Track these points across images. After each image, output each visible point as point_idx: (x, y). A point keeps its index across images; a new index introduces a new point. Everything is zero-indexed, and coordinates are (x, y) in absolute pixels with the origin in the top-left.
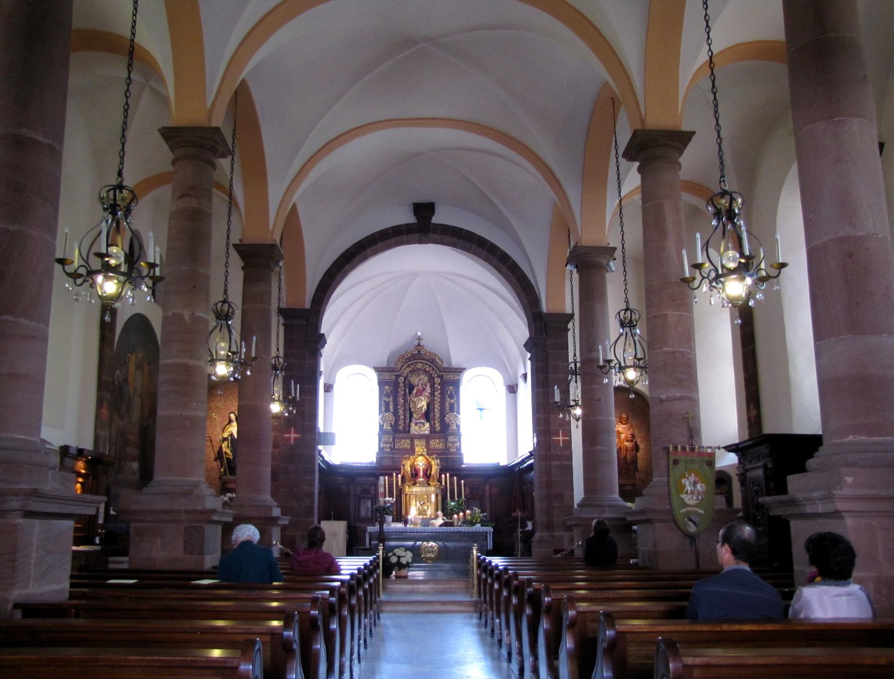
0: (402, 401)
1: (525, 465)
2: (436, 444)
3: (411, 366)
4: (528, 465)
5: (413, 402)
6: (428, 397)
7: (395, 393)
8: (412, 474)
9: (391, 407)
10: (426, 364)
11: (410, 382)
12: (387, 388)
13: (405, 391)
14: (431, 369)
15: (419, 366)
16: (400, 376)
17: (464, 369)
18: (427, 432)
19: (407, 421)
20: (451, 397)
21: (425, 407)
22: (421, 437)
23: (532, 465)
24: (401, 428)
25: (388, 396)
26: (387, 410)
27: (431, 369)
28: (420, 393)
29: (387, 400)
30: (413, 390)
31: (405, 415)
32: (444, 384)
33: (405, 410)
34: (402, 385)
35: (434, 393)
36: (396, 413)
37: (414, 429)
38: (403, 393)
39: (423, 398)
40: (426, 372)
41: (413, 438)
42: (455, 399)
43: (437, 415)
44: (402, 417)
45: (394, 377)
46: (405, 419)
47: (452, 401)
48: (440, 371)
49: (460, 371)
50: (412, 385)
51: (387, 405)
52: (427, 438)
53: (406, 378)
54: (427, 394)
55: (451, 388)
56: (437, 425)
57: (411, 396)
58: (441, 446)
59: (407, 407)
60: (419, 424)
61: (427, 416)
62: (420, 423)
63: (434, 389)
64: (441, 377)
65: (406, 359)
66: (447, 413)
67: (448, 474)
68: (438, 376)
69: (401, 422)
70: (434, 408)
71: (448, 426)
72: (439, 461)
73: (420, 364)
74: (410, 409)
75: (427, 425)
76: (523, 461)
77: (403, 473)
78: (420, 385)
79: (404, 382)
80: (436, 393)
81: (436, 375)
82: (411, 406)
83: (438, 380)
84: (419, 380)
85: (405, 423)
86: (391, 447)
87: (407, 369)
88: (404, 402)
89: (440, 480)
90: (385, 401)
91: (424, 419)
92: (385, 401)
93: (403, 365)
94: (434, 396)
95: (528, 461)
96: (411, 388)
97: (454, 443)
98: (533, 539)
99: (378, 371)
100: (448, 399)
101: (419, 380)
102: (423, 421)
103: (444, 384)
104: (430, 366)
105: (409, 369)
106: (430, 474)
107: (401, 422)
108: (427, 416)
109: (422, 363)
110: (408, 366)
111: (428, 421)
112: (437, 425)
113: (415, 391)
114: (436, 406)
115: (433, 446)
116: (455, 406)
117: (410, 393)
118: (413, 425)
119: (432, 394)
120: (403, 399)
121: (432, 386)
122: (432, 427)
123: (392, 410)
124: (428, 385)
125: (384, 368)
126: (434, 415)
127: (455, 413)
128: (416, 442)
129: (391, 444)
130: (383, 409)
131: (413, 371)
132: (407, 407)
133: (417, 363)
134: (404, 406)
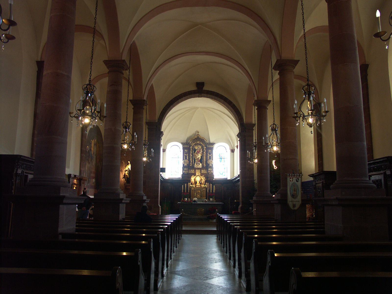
0: (192, 155)
1: (237, 180)
2: (203, 171)
3: (195, 142)
4: (238, 180)
5: (196, 156)
6: (201, 154)
8: (195, 183)
10: (201, 142)
11: (194, 148)
13: (193, 152)
14: (202, 143)
15: (198, 142)
17: (215, 143)
18: (200, 167)
19: (193, 163)
20: (210, 154)
21: (200, 158)
22: (198, 169)
23: (239, 179)
25: (186, 153)
26: (186, 159)
27: (202, 143)
28: (198, 152)
29: (186, 155)
30: (196, 151)
31: (192, 161)
33: (192, 159)
35: (203, 153)
36: (189, 160)
38: (192, 152)
39: (199, 154)
40: (200, 145)
41: (195, 169)
42: (211, 155)
43: (205, 160)
44: (192, 161)
46: (192, 162)
47: (210, 155)
48: (206, 144)
49: (213, 144)
50: (195, 149)
51: (186, 156)
53: (193, 147)
54: (201, 153)
55: (210, 150)
57: (195, 153)
59: (193, 158)
60: (198, 164)
61: (201, 161)
62: (198, 163)
63: (203, 150)
64: (206, 146)
65: (194, 140)
66: (208, 160)
67: (208, 183)
69: (191, 163)
70: (203, 158)
71: (209, 165)
72: (205, 178)
73: (198, 142)
74: (194, 158)
75: (201, 164)
76: (236, 178)
77: (191, 183)
78: (198, 149)
79: (192, 149)
80: (204, 152)
81: (204, 146)
82: (195, 157)
83: (205, 148)
84: (198, 148)
85: (192, 163)
86: (187, 172)
87: (194, 143)
88: (192, 156)
90: (185, 155)
91: (199, 162)
92: (185, 155)
93: (192, 142)
94: (204, 154)
95: (238, 178)
96: (195, 150)
97: (210, 171)
98: (239, 207)
99: (183, 144)
100: (209, 155)
101: (198, 148)
102: (199, 163)
103: (208, 149)
104: (202, 142)
106: (201, 183)
107: (191, 163)
108: (201, 161)
109: (199, 141)
110: (194, 142)
113: (196, 152)
114: (204, 157)
115: (203, 172)
116: (211, 157)
117: (194, 152)
118: (195, 164)
119: (203, 153)
120: (192, 155)
122: (203, 165)
123: (188, 159)
124: (201, 150)
125: (185, 143)
126: (203, 161)
127: (211, 160)
128: (197, 171)
129: (187, 171)
131: (196, 145)
132: (193, 158)
133: (197, 141)
134: (192, 157)
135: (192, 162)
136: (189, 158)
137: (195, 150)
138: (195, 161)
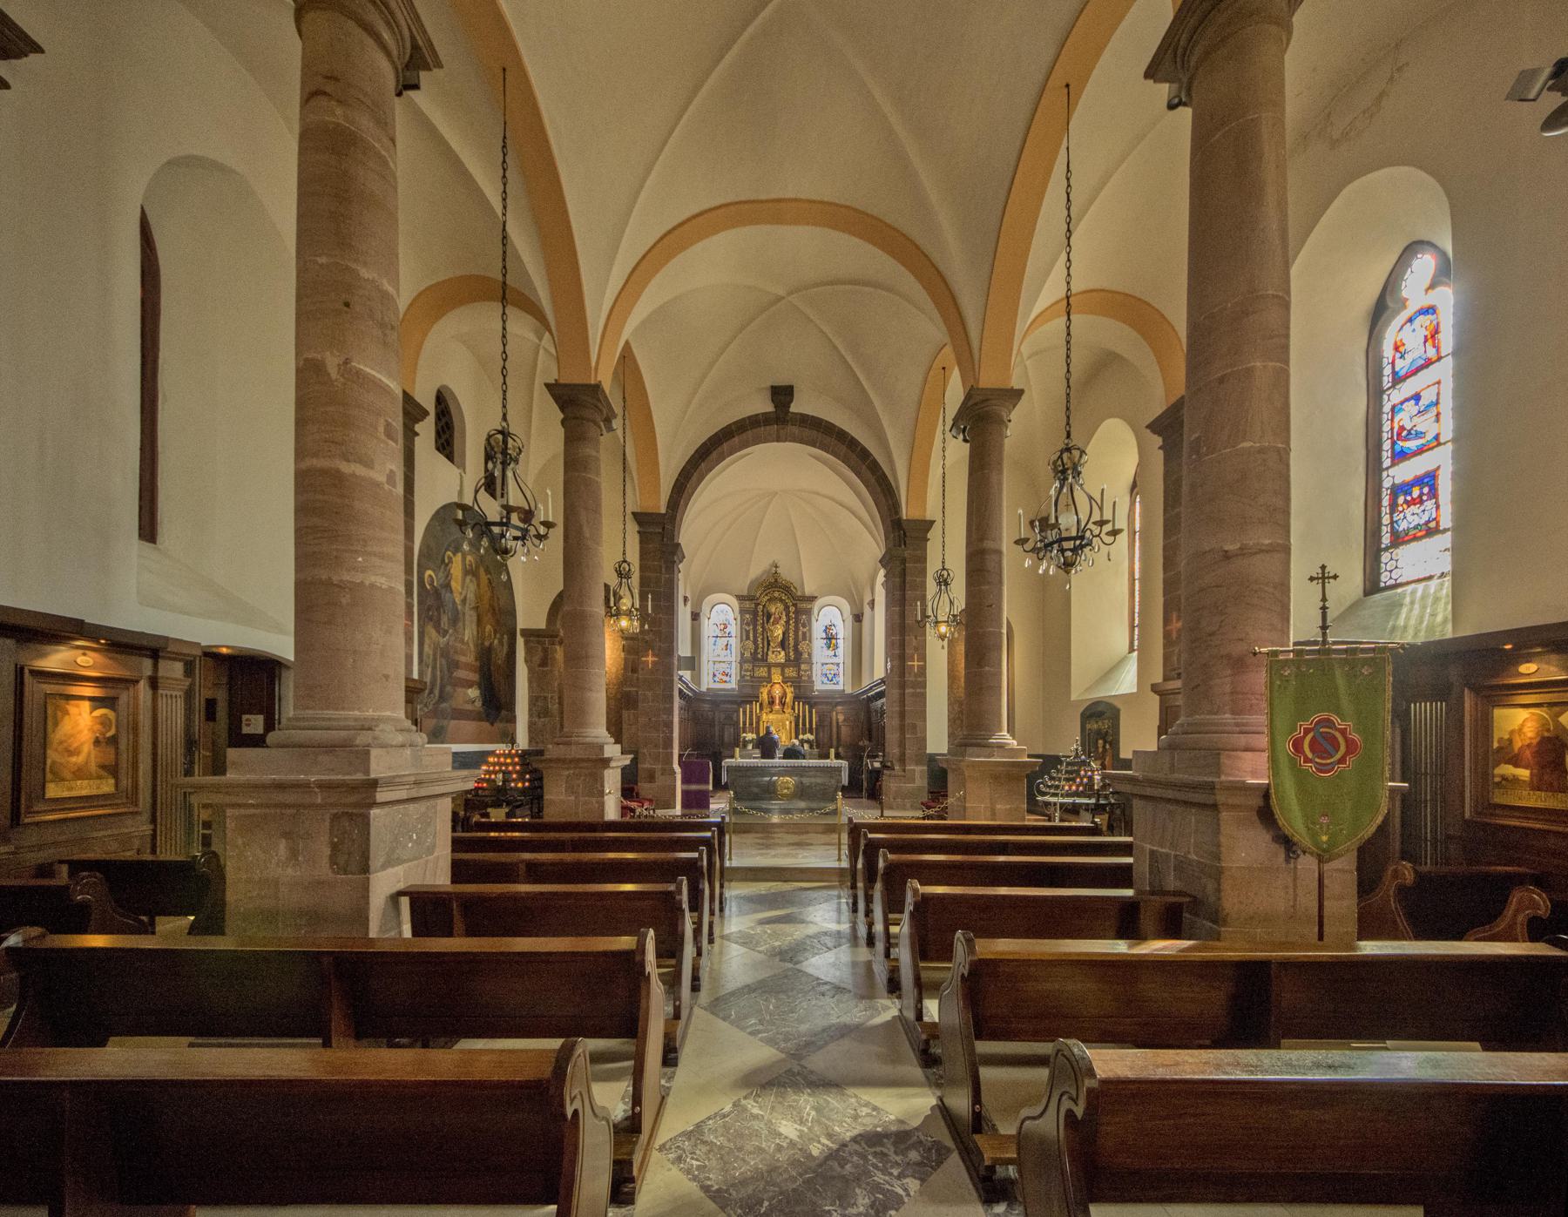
2: (791, 672)
7: (754, 621)
9: (751, 635)
12: (748, 616)
15: (776, 594)
16: (759, 604)
24: (759, 656)
25: (748, 624)
28: (776, 622)
32: (797, 612)
33: (763, 639)
34: (760, 613)
37: (772, 658)
40: (781, 600)
41: (769, 666)
45: (753, 606)
46: (763, 648)
52: (782, 666)
53: (764, 606)
56: (791, 654)
58: (794, 674)
61: (783, 645)
68: (793, 605)
75: (783, 653)
83: (792, 609)
89: (793, 709)
96: (769, 616)
105: (767, 598)
107: (760, 650)
108: (783, 645)
111: (783, 649)
112: (791, 654)
113: (772, 620)
117: (768, 621)
118: (770, 653)
119: (787, 622)
121: (787, 615)
122: (787, 655)
130: (744, 638)
135: (763, 648)
136: (755, 637)
137: (769, 616)
138: (769, 644)
